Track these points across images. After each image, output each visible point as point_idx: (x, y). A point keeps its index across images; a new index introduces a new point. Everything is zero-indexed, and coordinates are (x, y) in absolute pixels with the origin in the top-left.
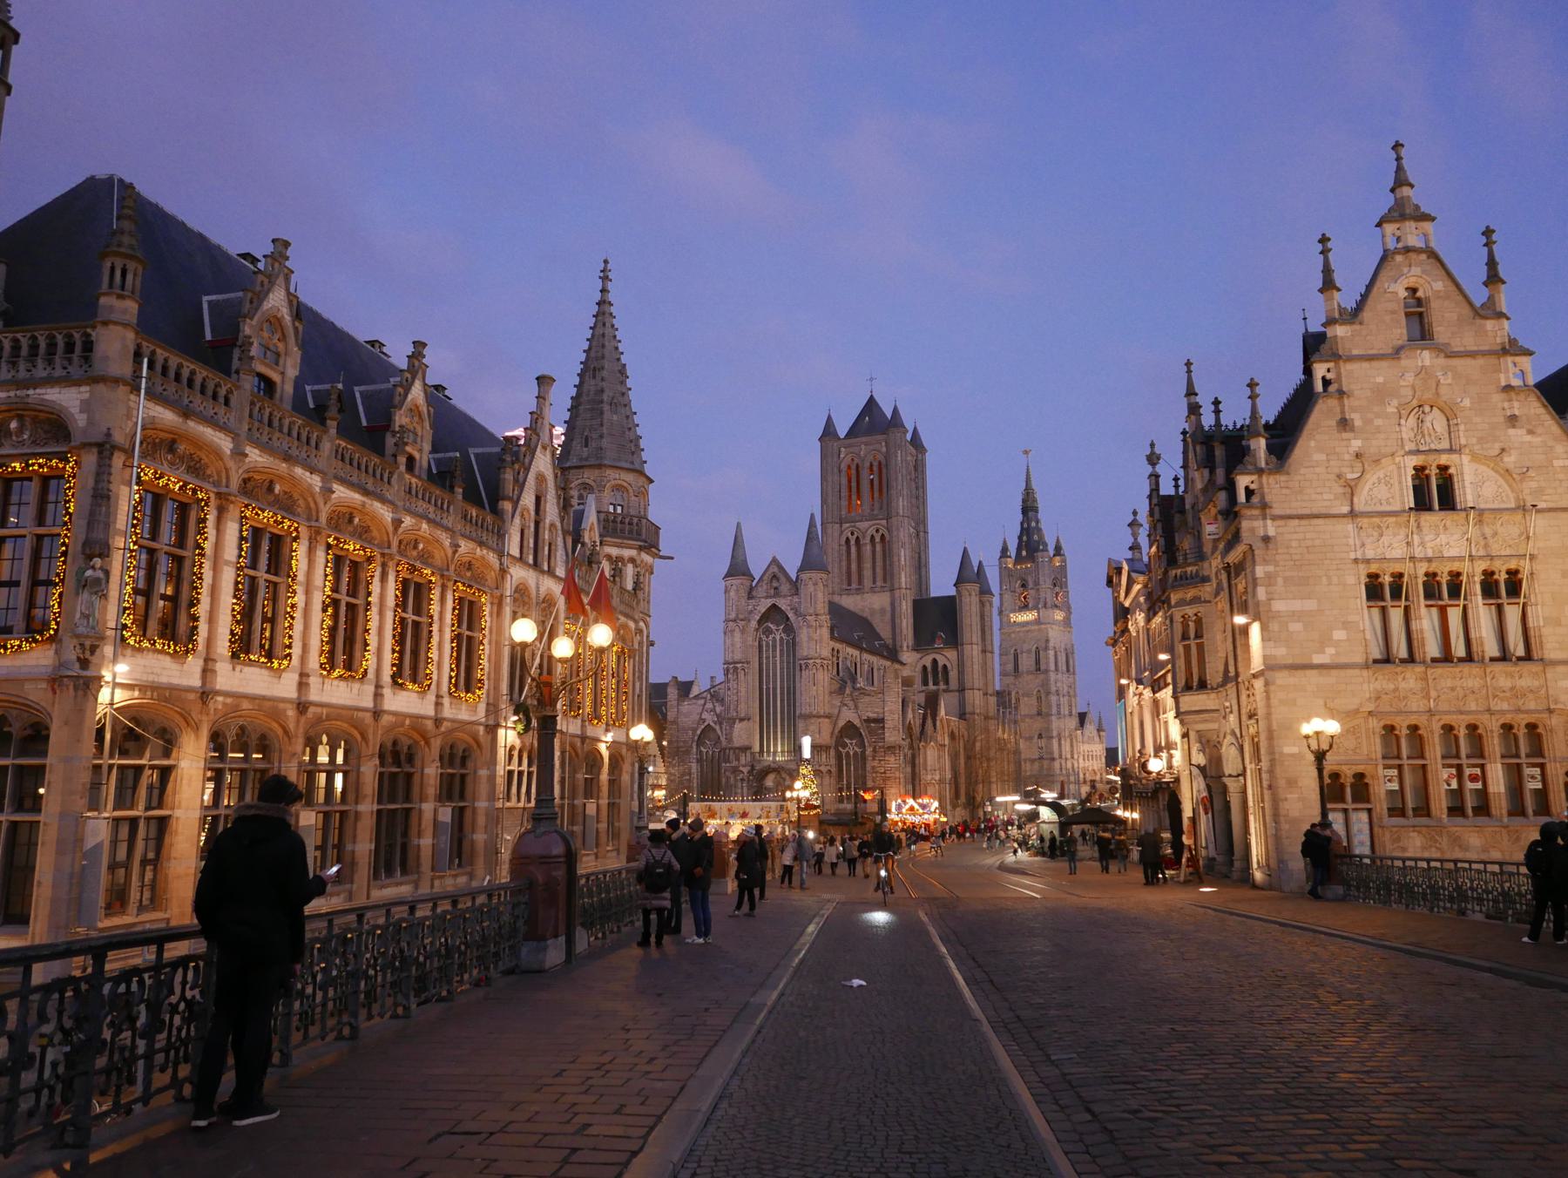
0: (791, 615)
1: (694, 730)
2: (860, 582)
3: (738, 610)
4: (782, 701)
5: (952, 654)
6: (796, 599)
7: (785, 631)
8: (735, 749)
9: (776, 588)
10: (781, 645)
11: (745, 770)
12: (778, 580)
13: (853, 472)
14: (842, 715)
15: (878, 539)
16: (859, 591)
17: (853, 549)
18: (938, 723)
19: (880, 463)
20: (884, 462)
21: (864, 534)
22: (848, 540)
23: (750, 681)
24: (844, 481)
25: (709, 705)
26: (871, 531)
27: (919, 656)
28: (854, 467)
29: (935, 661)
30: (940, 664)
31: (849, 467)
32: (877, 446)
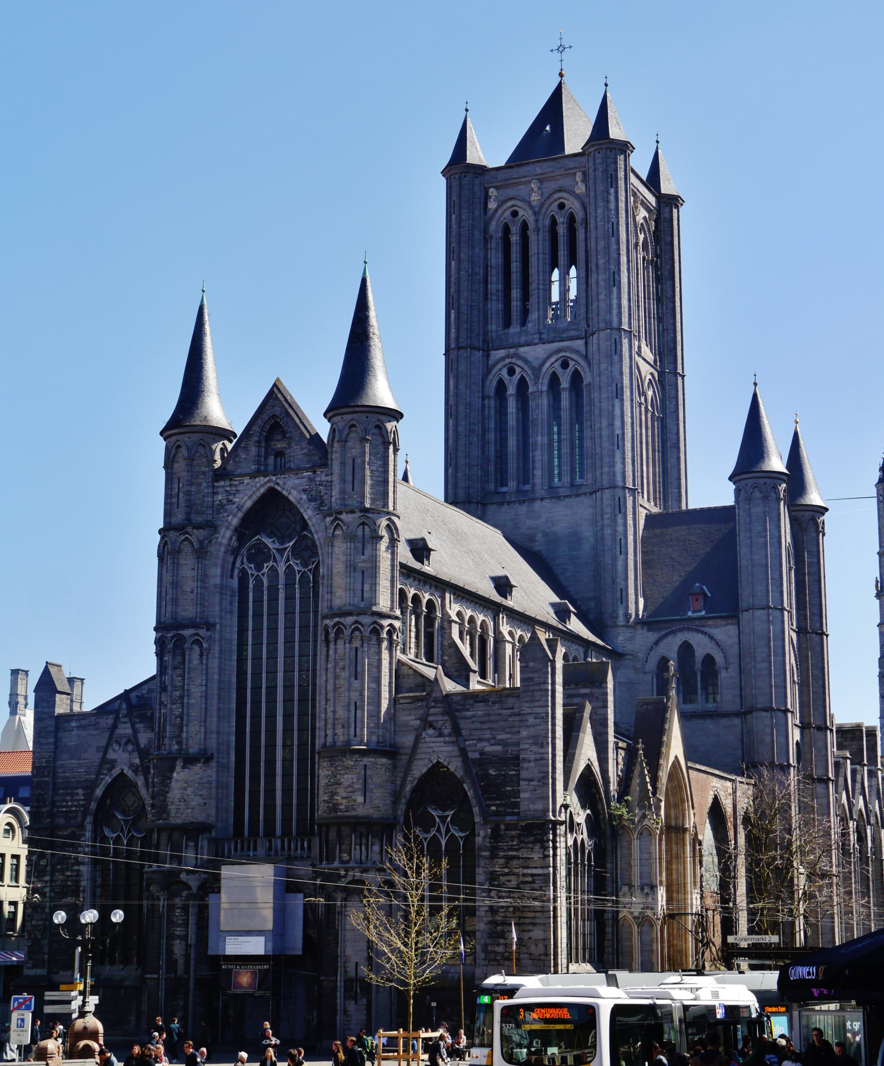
0: (308, 513)
1: (90, 787)
2: (525, 475)
3: (190, 505)
4: (288, 716)
5: (725, 633)
6: (321, 477)
7: (295, 552)
8: (173, 829)
9: (279, 454)
10: (289, 586)
11: (194, 883)
12: (284, 433)
13: (515, 238)
14: (423, 748)
15: (565, 383)
16: (525, 497)
17: (512, 406)
18: (663, 775)
19: (572, 218)
20: (579, 215)
21: (537, 371)
22: (501, 386)
23: (214, 663)
24: (496, 258)
25: (125, 729)
26: (552, 365)
27: (652, 637)
28: (515, 229)
29: (686, 649)
30: (699, 654)
31: (506, 230)
32: (566, 182)
